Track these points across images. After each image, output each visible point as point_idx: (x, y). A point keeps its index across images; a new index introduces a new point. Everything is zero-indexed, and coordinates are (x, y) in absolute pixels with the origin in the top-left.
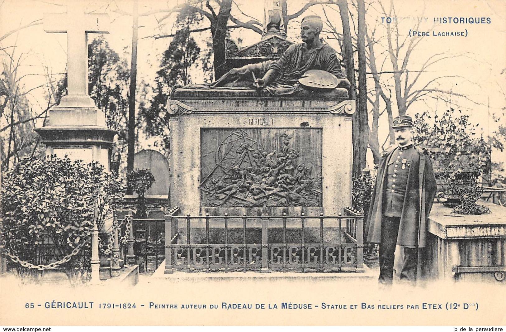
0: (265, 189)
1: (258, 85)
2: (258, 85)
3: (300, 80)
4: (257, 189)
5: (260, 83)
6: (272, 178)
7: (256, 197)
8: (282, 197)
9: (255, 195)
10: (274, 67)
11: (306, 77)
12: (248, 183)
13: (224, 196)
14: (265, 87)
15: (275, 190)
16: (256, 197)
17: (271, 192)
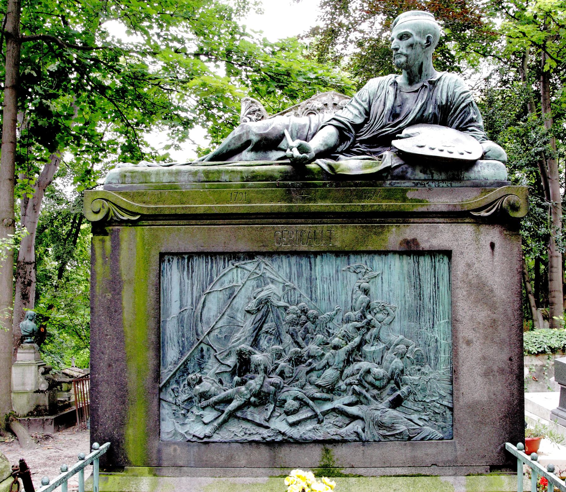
0: (313, 399)
1: (296, 153)
2: (296, 153)
3: (395, 143)
4: (296, 399)
5: (301, 149)
6: (330, 374)
7: (292, 419)
8: (354, 418)
9: (288, 413)
11: (409, 136)
12: (272, 385)
13: (214, 414)
14: (314, 159)
15: (338, 403)
16: (292, 419)
17: (328, 406)
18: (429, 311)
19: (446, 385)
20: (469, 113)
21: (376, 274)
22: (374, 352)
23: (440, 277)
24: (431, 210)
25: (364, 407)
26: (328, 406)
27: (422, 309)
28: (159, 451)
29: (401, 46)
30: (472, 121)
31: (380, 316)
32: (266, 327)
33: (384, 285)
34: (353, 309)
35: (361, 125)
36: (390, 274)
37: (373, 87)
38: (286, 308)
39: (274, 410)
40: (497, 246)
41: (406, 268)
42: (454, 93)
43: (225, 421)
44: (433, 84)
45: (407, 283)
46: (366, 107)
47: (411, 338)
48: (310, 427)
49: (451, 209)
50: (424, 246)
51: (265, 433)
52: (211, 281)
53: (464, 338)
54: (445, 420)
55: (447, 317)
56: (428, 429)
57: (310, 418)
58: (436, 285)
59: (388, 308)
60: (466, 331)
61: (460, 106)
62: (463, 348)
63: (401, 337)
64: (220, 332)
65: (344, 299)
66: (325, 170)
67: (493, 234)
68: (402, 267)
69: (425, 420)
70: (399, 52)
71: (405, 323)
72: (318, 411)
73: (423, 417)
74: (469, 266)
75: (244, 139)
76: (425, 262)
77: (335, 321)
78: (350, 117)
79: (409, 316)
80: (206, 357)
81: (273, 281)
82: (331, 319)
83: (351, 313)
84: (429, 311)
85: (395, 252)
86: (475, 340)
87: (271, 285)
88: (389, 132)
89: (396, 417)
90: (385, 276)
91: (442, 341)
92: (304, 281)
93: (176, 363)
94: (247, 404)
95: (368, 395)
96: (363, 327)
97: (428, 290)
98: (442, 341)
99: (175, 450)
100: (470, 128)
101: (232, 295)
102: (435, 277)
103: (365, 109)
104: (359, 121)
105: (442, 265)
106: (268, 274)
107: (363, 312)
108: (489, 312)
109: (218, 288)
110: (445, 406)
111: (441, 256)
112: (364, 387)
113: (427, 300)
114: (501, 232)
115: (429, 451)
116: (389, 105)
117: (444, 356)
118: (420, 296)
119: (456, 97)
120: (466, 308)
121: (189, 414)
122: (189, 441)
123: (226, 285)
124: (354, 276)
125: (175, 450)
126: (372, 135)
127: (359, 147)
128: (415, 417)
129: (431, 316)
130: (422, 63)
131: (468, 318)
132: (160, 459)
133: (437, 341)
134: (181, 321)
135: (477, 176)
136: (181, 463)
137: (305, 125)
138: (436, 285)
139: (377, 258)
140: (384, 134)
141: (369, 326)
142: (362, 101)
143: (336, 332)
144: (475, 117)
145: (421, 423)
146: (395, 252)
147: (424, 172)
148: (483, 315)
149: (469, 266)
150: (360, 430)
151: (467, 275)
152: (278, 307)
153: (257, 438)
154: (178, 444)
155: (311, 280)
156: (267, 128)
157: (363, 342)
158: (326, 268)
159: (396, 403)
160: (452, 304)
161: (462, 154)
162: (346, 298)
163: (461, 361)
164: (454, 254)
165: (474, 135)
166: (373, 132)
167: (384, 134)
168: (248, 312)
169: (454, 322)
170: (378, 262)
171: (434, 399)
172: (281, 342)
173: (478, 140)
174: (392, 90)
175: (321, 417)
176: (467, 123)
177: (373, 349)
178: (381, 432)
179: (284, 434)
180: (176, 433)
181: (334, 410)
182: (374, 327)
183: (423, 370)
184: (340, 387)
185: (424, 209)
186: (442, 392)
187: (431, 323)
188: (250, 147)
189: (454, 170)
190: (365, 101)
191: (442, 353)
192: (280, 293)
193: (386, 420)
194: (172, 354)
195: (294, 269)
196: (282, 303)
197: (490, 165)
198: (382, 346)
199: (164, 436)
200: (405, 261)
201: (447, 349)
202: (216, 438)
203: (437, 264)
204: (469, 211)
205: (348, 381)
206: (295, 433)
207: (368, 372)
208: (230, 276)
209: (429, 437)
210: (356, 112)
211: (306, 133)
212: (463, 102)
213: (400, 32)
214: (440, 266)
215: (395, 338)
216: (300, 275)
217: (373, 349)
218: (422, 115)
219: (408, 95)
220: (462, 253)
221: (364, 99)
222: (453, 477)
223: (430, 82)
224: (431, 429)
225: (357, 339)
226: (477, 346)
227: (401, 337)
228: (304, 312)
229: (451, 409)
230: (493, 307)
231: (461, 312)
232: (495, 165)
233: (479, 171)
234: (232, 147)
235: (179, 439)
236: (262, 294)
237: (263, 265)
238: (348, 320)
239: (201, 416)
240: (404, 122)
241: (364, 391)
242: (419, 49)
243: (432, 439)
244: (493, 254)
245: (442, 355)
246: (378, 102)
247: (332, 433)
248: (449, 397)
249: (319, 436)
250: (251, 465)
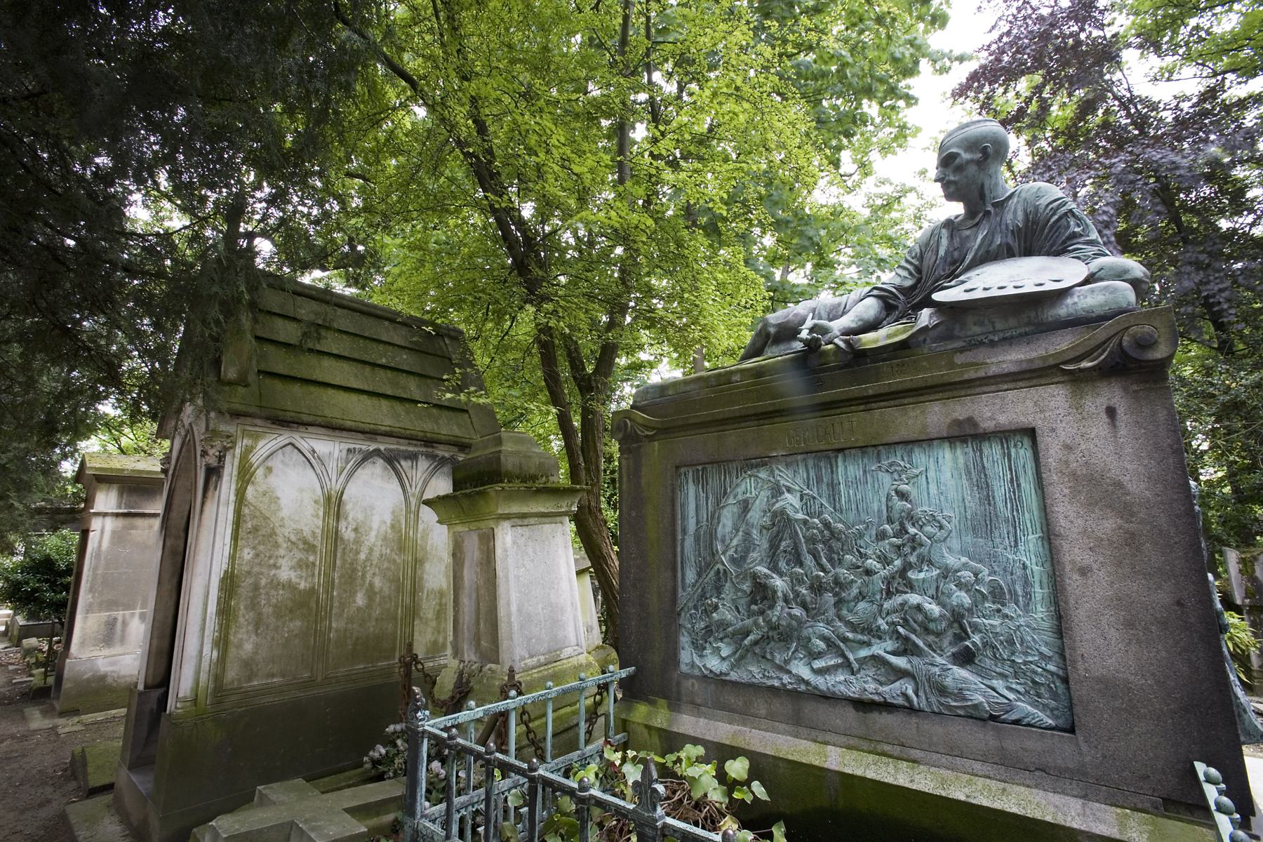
0: (845, 640)
3: (937, 296)
7: (818, 664)
9: (814, 655)
10: (875, 292)
15: (878, 649)
16: (818, 664)
17: (864, 653)
18: (1007, 521)
19: (1048, 637)
20: (1069, 226)
21: (916, 471)
22: (924, 580)
23: (1020, 469)
24: (990, 373)
25: (916, 660)
26: (864, 653)
27: (994, 519)
28: (678, 684)
30: (1074, 235)
31: (928, 529)
32: (783, 543)
33: (931, 486)
34: (890, 521)
35: (913, 288)
36: (938, 470)
38: (805, 522)
39: (796, 650)
40: (1120, 411)
41: (961, 460)
42: (1037, 208)
43: (742, 657)
44: (1000, 205)
45: (965, 482)
47: (980, 561)
48: (842, 678)
49: (1025, 366)
50: (988, 425)
51: (786, 679)
52: (725, 493)
53: (1073, 562)
54: (1054, 695)
55: (1039, 530)
56: (1025, 708)
57: (836, 667)
58: (1015, 482)
59: (940, 518)
60: (1074, 553)
62: (1073, 581)
63: (964, 559)
64: (736, 552)
65: (875, 506)
67: (1111, 394)
68: (955, 459)
69: (1019, 692)
71: (969, 539)
72: (851, 657)
73: (1014, 686)
74: (1068, 448)
76: (993, 452)
77: (867, 539)
78: (898, 281)
79: (974, 530)
80: (723, 579)
81: (789, 490)
82: (861, 535)
83: (887, 526)
84: (1007, 521)
85: (942, 439)
86: (1095, 566)
87: (787, 495)
89: (965, 681)
90: (931, 474)
91: (1035, 568)
92: (825, 487)
93: (694, 586)
94: (765, 639)
95: (921, 644)
96: (904, 545)
97: (1000, 491)
98: (1035, 568)
99: (693, 685)
101: (745, 506)
102: (1010, 469)
103: (916, 267)
104: (909, 283)
105: (1022, 452)
106: (782, 482)
107: (902, 524)
108: (1119, 521)
109: (731, 501)
110: (1052, 674)
111: (1018, 438)
112: (914, 632)
113: (1000, 505)
114: (1125, 389)
115: (1029, 744)
116: (942, 252)
117: (1039, 592)
118: (988, 499)
120: (1072, 515)
121: (708, 645)
122: (706, 676)
123: (740, 497)
124: (886, 479)
125: (693, 685)
128: (998, 684)
129: (1011, 529)
130: (983, 185)
131: (1076, 530)
132: (679, 693)
133: (1025, 567)
134: (697, 539)
135: (1071, 310)
136: (699, 701)
138: (1015, 482)
139: (917, 450)
141: (914, 543)
143: (869, 552)
144: (1077, 230)
145: (1011, 696)
146: (942, 439)
147: (982, 324)
148: (1109, 525)
149: (1068, 448)
150: (910, 692)
151: (1067, 463)
152: (796, 520)
153: (776, 683)
154: (696, 677)
155: (833, 486)
157: (907, 566)
158: (851, 468)
159: (966, 658)
160: (1045, 509)
162: (880, 507)
163: (1072, 602)
164: (1039, 432)
168: (764, 527)
169: (1049, 536)
170: (920, 458)
171: (1030, 659)
172: (801, 565)
175: (856, 666)
176: (1064, 242)
177: (922, 575)
178: (943, 700)
179: (807, 683)
180: (693, 665)
181: (873, 657)
182: (921, 545)
183: (1006, 611)
184: (879, 627)
185: (981, 374)
186: (1044, 649)
187: (1012, 539)
189: (1030, 310)
191: (1037, 586)
192: (797, 504)
193: (949, 682)
194: (691, 576)
195: (812, 474)
196: (800, 516)
198: (935, 572)
199: (684, 668)
200: (959, 451)
201: (1045, 581)
202: (734, 676)
203: (1013, 451)
204: (1057, 366)
205: (889, 619)
206: (820, 682)
207: (919, 608)
208: (743, 487)
209: (1026, 720)
210: (904, 273)
214: (1017, 453)
215: (952, 560)
216: (819, 480)
217: (922, 575)
220: (1053, 430)
222: (1080, 801)
223: (995, 205)
224: (1029, 708)
225: (898, 563)
226: (1101, 576)
227: (964, 559)
228: (827, 525)
229: (1065, 680)
230: (1126, 511)
231: (1063, 522)
232: (1106, 288)
233: (1075, 303)
234: (758, 345)
235: (696, 672)
236: (777, 505)
237: (777, 472)
238: (882, 536)
239: (718, 649)
241: (913, 637)
242: (973, 169)
243: (1032, 726)
244: (1114, 426)
245: (1038, 589)
247: (871, 690)
248: (1056, 657)
249: (853, 691)
250: (771, 716)
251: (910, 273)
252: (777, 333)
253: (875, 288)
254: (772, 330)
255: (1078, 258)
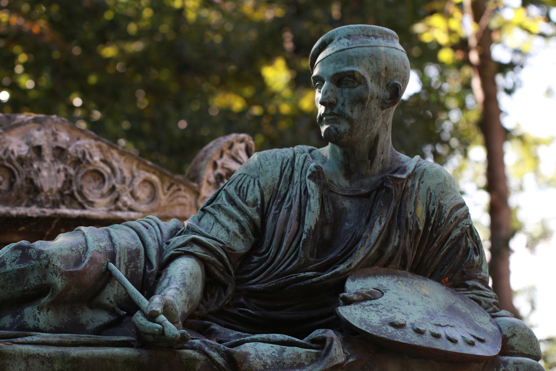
10: (196, 249)
20: (467, 250)
29: (341, 100)
37: (269, 175)
46: (257, 217)
61: (450, 234)
66: (218, 365)
70: (335, 111)
75: (33, 280)
78: (223, 235)
88: (314, 280)
100: (470, 283)
104: (240, 246)
116: (311, 219)
119: (446, 216)
126: (273, 283)
127: (243, 306)
130: (377, 138)
137: (137, 251)
140: (302, 284)
142: (246, 204)
156: (79, 261)
161: (472, 344)
165: (478, 297)
166: (277, 277)
167: (302, 284)
173: (486, 309)
174: (312, 185)
188: (45, 300)
190: (254, 204)
197: (520, 366)
210: (234, 227)
211: (141, 270)
212: (456, 226)
213: (339, 71)
218: (381, 251)
219: (347, 204)
221: (250, 198)
240: (346, 264)
246: (284, 211)
251: (242, 229)
252: (67, 289)
253: (195, 241)
254: (59, 282)
255: (479, 302)
